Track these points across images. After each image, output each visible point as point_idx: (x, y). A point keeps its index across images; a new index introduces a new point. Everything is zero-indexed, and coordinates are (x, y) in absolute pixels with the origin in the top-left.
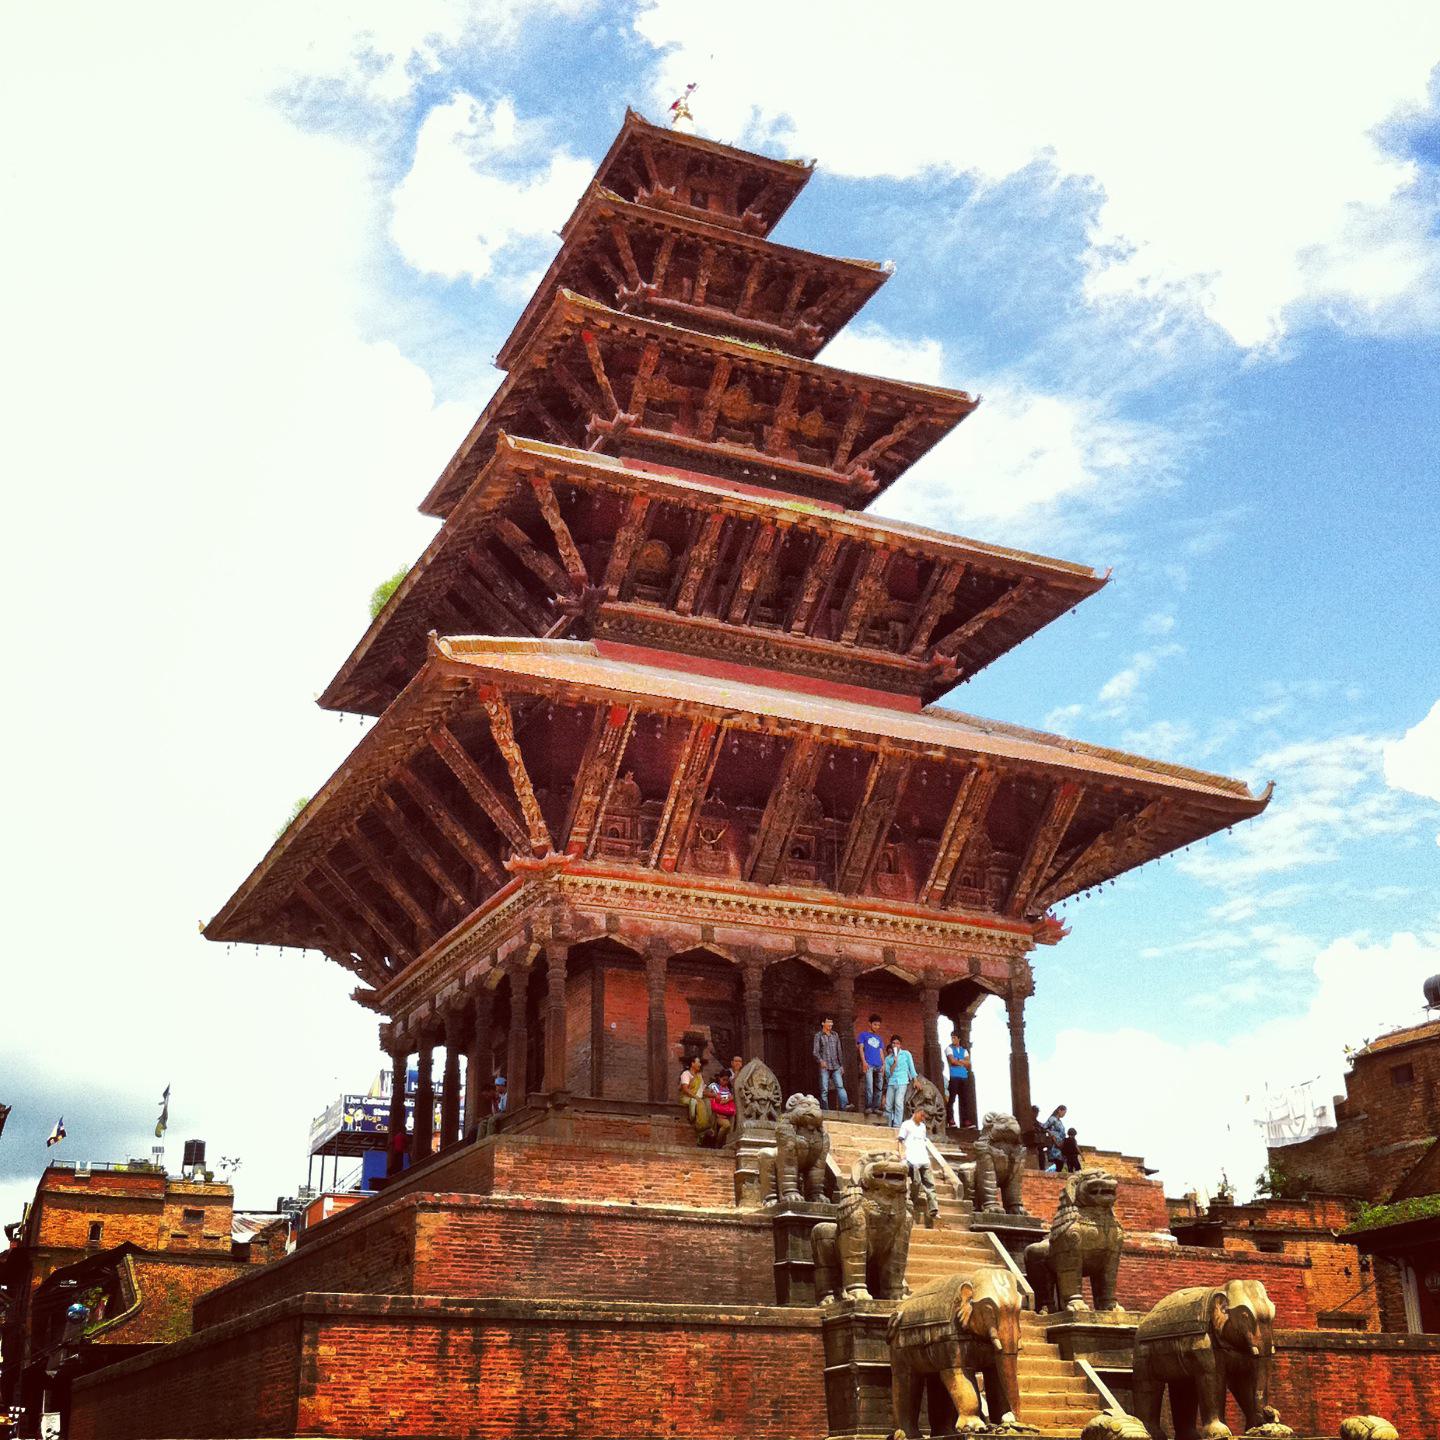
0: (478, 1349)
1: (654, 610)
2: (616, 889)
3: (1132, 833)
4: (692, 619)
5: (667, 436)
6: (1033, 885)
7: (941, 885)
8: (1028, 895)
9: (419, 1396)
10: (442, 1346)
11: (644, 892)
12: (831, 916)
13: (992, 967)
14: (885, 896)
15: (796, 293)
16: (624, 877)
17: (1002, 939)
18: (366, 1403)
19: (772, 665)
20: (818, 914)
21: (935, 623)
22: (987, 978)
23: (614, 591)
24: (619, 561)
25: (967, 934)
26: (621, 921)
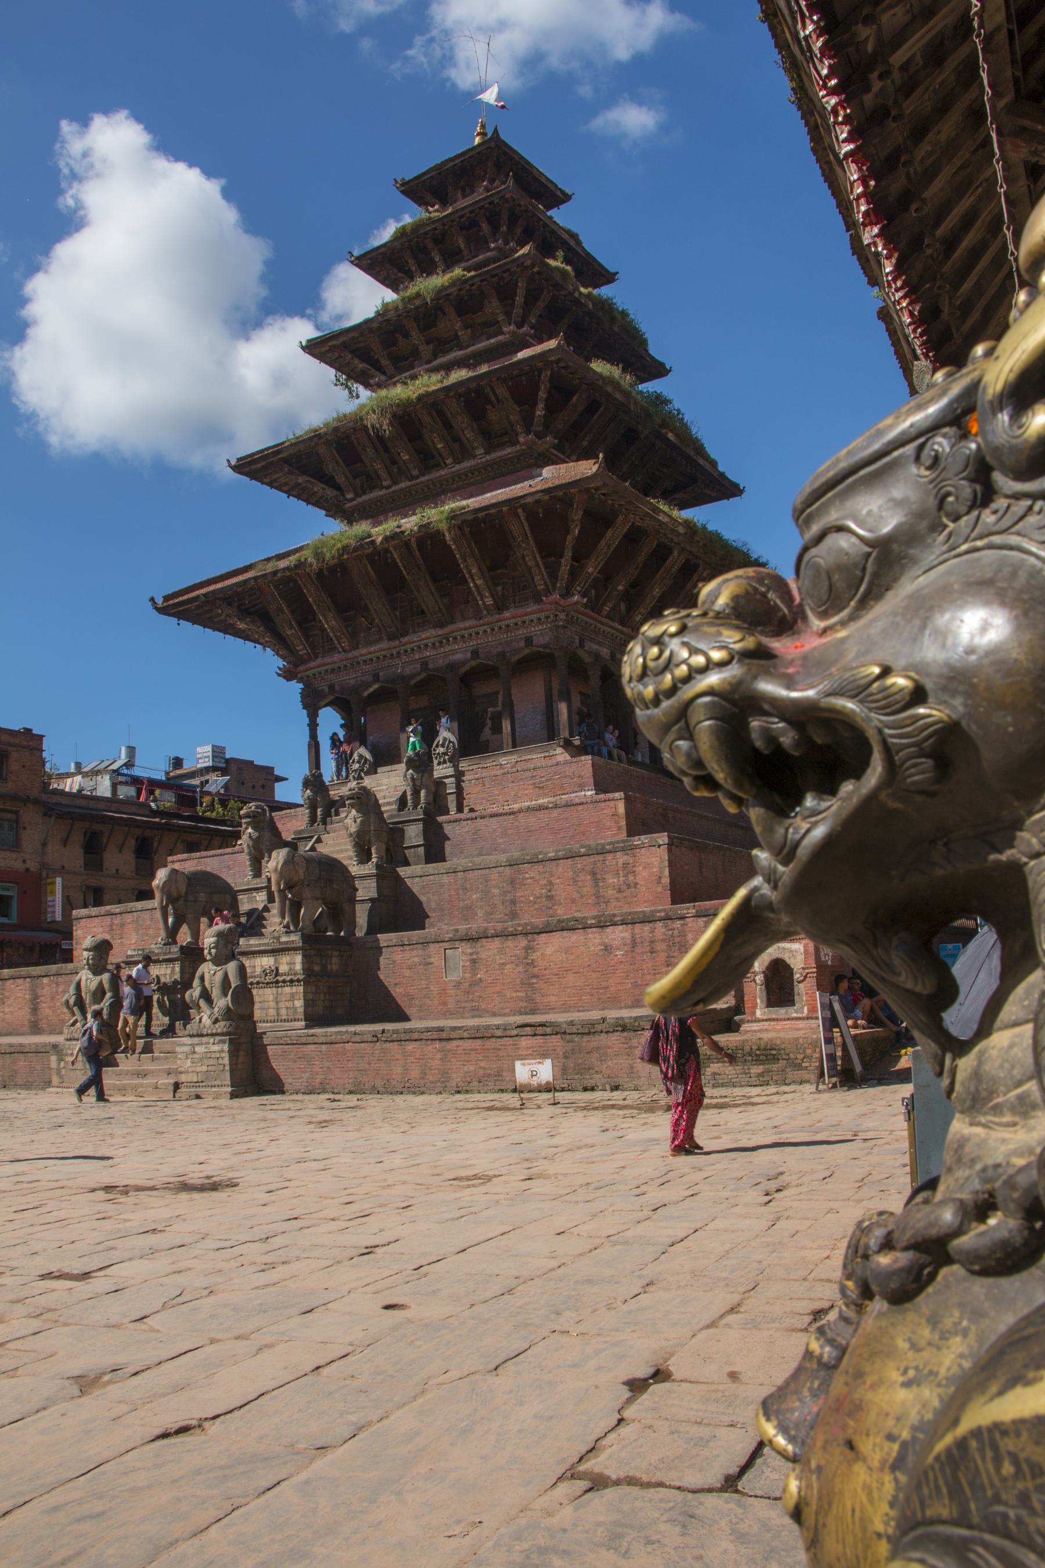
0: (122, 925)
2: (327, 671)
4: (393, 488)
6: (543, 579)
7: (489, 601)
8: (545, 584)
10: (111, 926)
11: (339, 668)
12: (434, 644)
14: (469, 618)
15: (485, 226)
17: (539, 619)
19: (444, 492)
23: (350, 496)
24: (341, 480)
25: (516, 624)
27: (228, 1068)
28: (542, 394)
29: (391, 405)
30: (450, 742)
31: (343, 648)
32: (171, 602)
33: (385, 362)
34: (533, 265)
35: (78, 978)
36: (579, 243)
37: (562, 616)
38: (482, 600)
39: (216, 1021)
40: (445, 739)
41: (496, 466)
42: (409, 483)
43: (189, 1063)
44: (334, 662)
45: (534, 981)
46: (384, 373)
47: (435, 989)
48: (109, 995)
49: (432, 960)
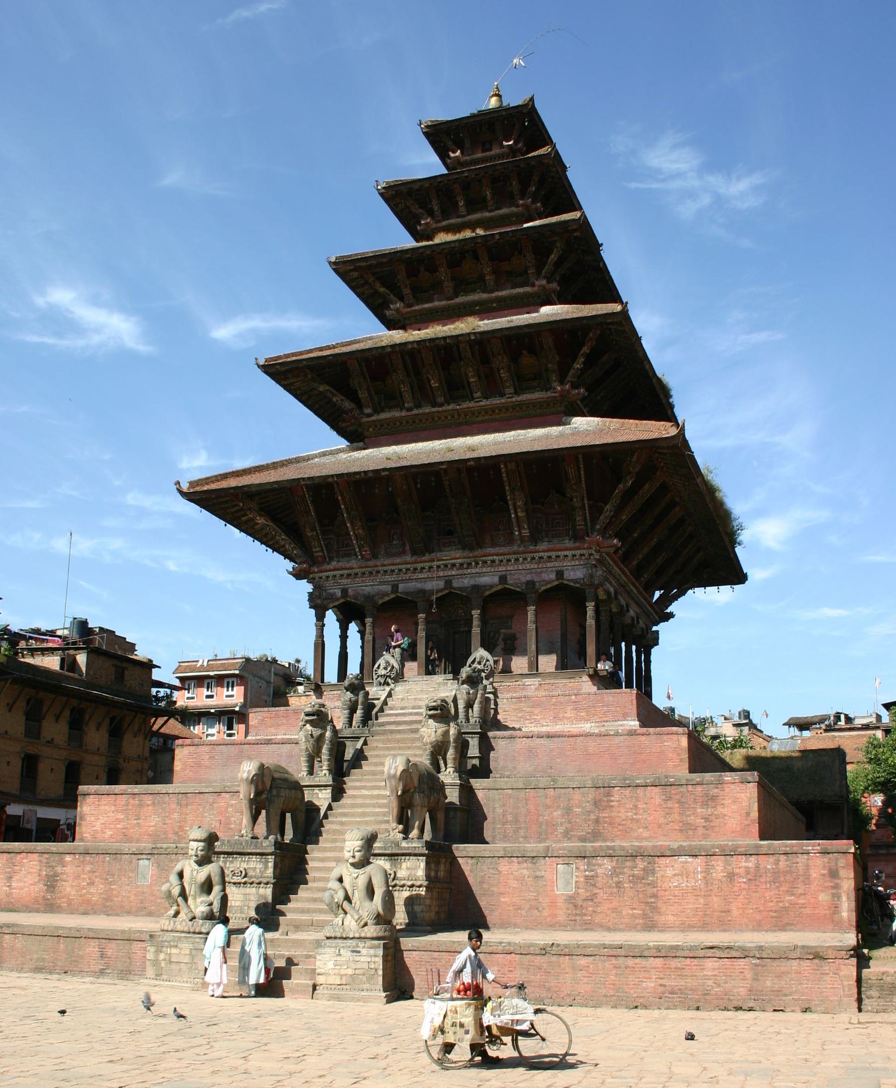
1: (396, 414)
2: (342, 575)
3: (630, 473)
4: (415, 412)
5: (426, 306)
7: (526, 532)
8: (586, 525)
9: (118, 826)
11: (356, 574)
12: (461, 565)
13: (572, 573)
16: (342, 569)
17: (574, 556)
18: (99, 829)
20: (454, 565)
21: (556, 367)
22: (568, 580)
24: (363, 395)
25: (550, 557)
26: (350, 590)
27: (380, 972)
28: (585, 350)
30: (487, 660)
31: (361, 555)
32: (198, 489)
33: (407, 291)
34: (575, 231)
35: (178, 868)
38: (520, 531)
39: (366, 924)
41: (524, 408)
43: (330, 965)
45: (653, 900)
46: (401, 299)
47: (545, 901)
48: (217, 889)
49: (543, 873)
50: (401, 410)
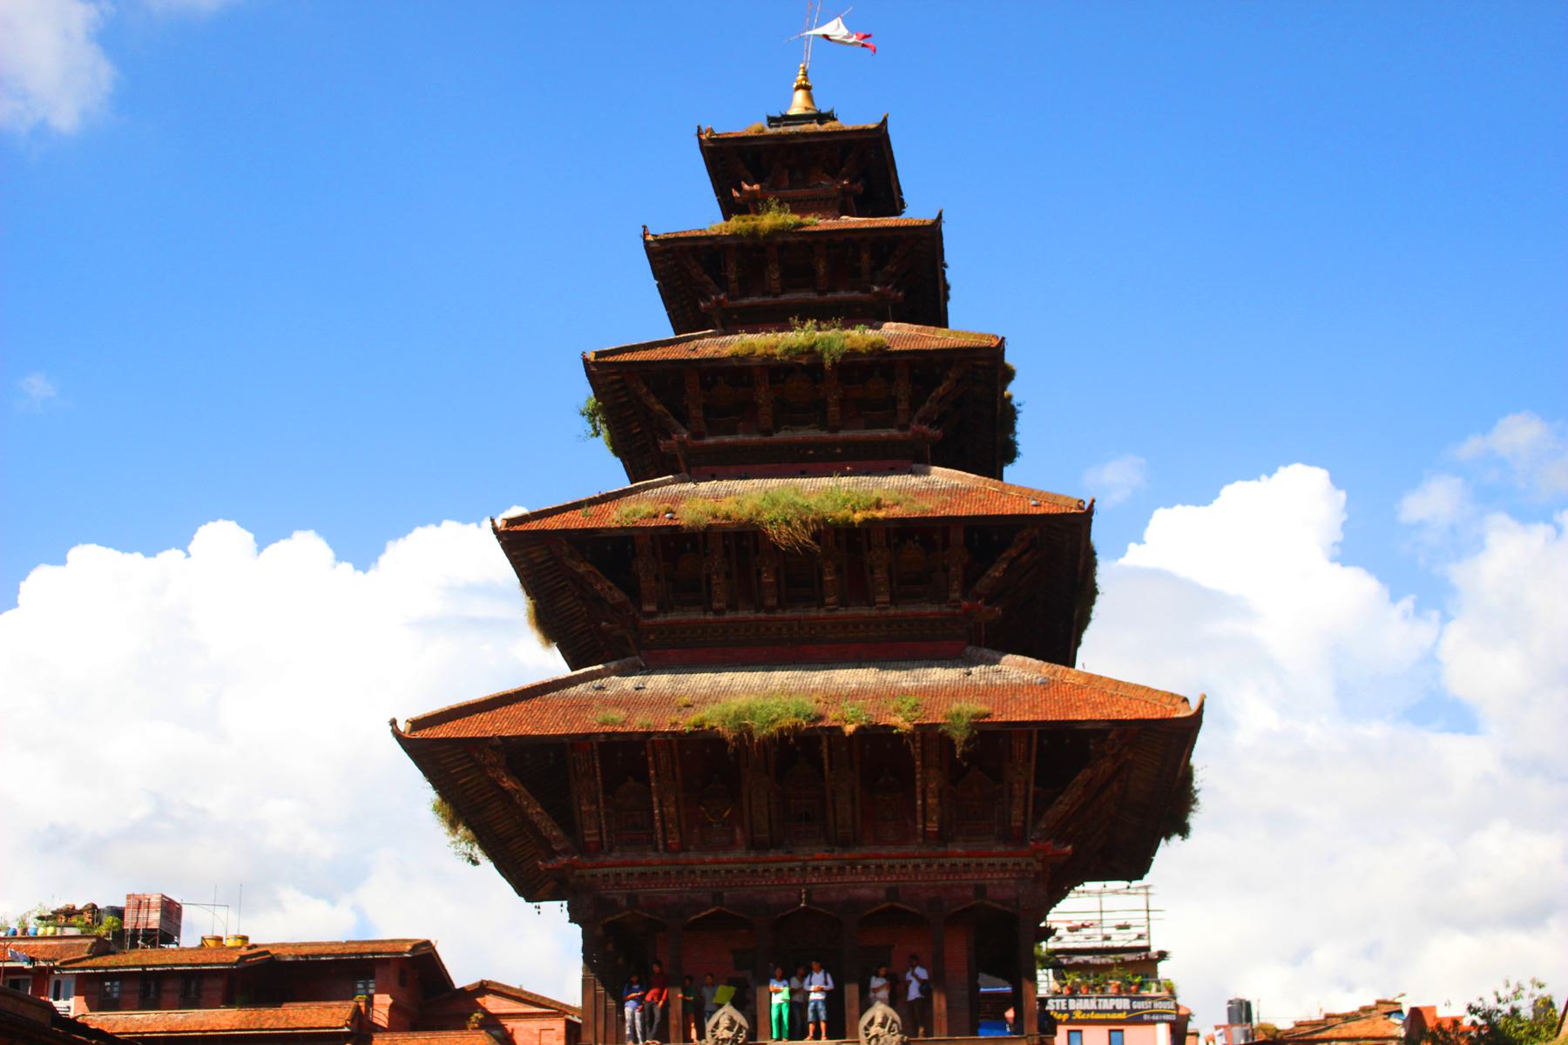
1: (695, 615)
2: (630, 874)
4: (729, 616)
5: (727, 439)
6: (1025, 814)
7: (933, 827)
8: (1025, 823)
12: (829, 869)
15: (865, 256)
16: (633, 864)
17: (1004, 865)
20: (816, 869)
25: (965, 865)
26: (640, 898)
29: (814, 521)
31: (665, 844)
36: (947, 298)
37: (1038, 867)
40: (885, 1019)
42: (762, 615)
44: (649, 864)
50: (705, 612)
